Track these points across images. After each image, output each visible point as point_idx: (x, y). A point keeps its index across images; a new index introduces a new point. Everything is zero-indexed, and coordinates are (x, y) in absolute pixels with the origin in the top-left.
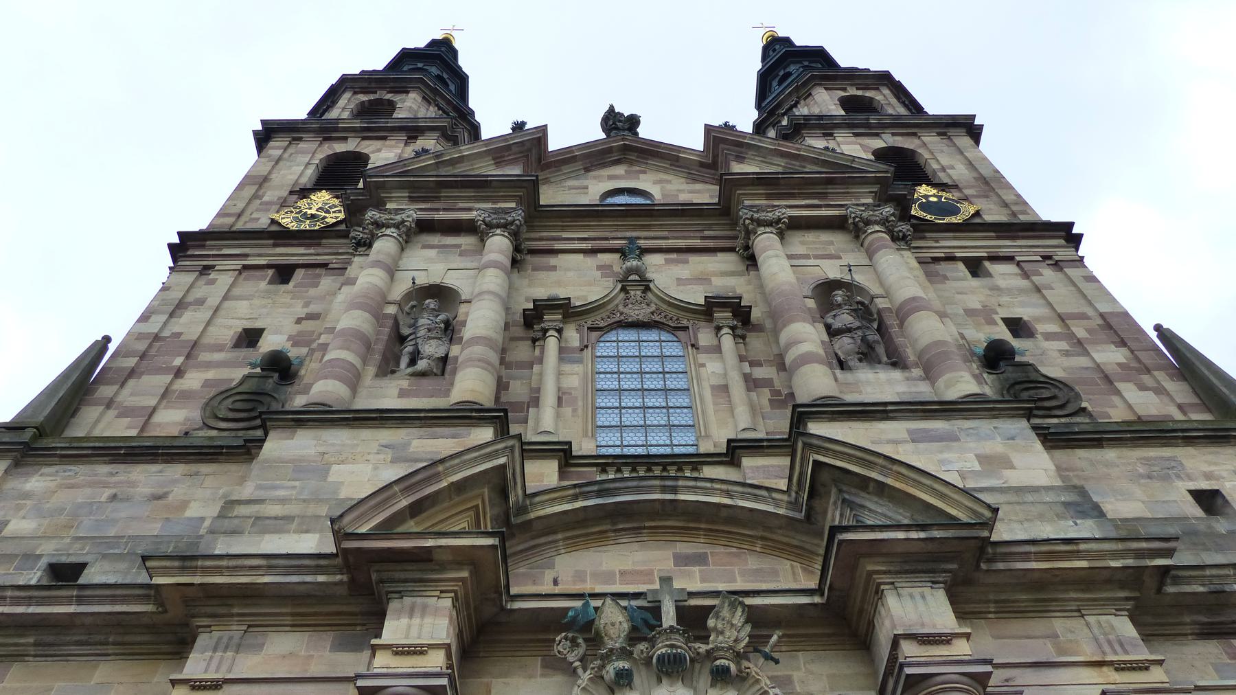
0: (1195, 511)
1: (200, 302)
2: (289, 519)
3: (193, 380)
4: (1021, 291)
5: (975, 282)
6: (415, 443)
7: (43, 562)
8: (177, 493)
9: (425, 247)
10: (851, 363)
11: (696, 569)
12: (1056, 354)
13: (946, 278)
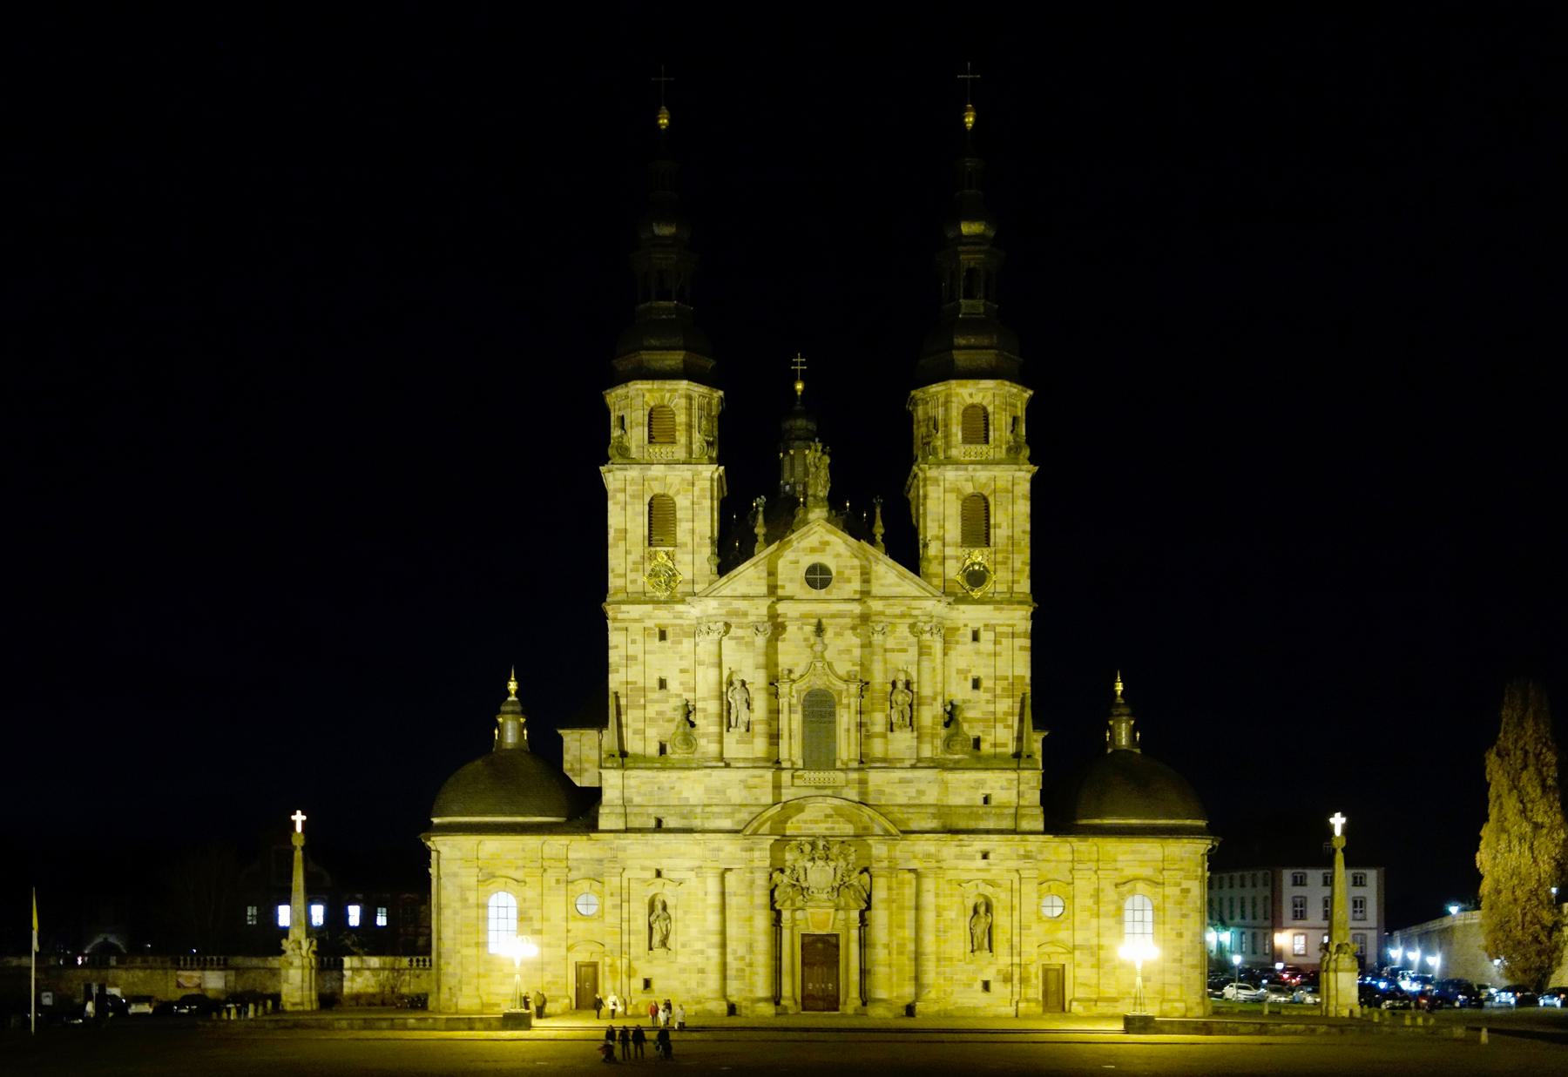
0: (980, 802)
1: (635, 658)
2: (720, 813)
3: (651, 711)
4: (989, 655)
5: (970, 646)
6: (750, 779)
7: (653, 817)
8: (677, 785)
9: (731, 638)
10: (894, 728)
11: (830, 819)
12: (983, 702)
13: (957, 643)
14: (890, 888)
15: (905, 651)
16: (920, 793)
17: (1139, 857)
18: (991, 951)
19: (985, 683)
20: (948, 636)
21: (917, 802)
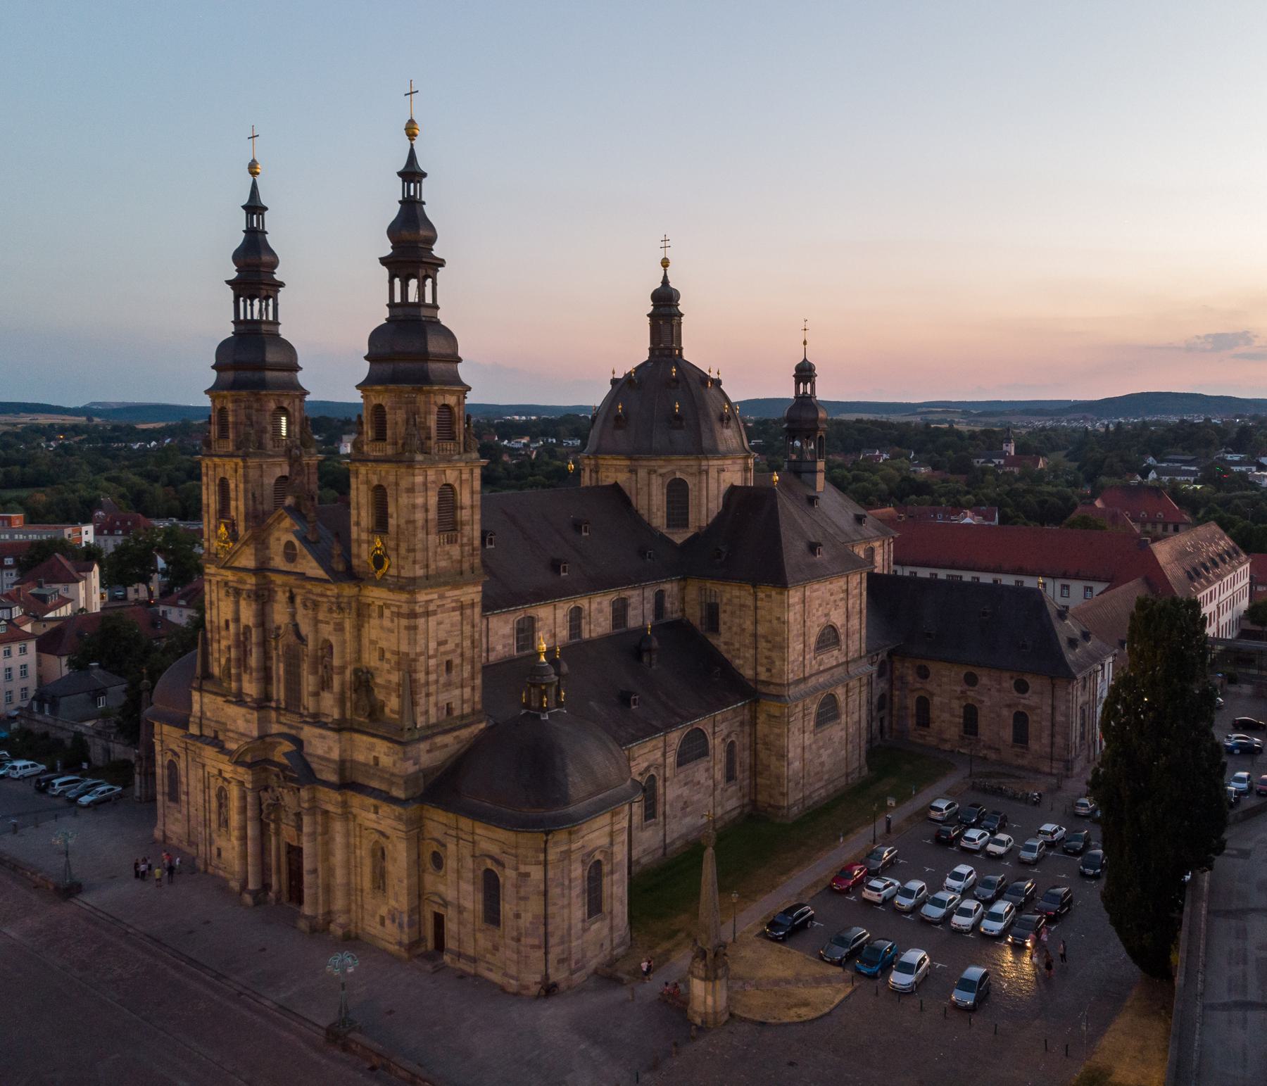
8: (225, 708)
13: (370, 616)
14: (315, 823)
15: (327, 623)
16: (330, 749)
17: (490, 834)
18: (384, 890)
19: (388, 655)
20: (362, 613)
21: (327, 756)
